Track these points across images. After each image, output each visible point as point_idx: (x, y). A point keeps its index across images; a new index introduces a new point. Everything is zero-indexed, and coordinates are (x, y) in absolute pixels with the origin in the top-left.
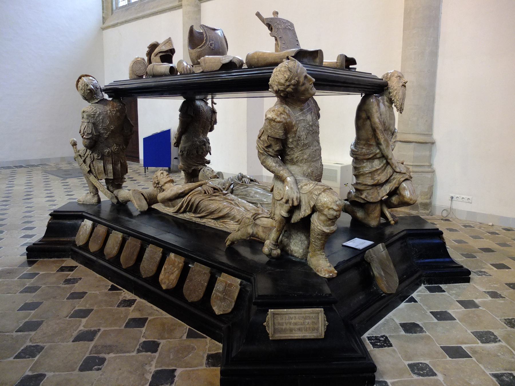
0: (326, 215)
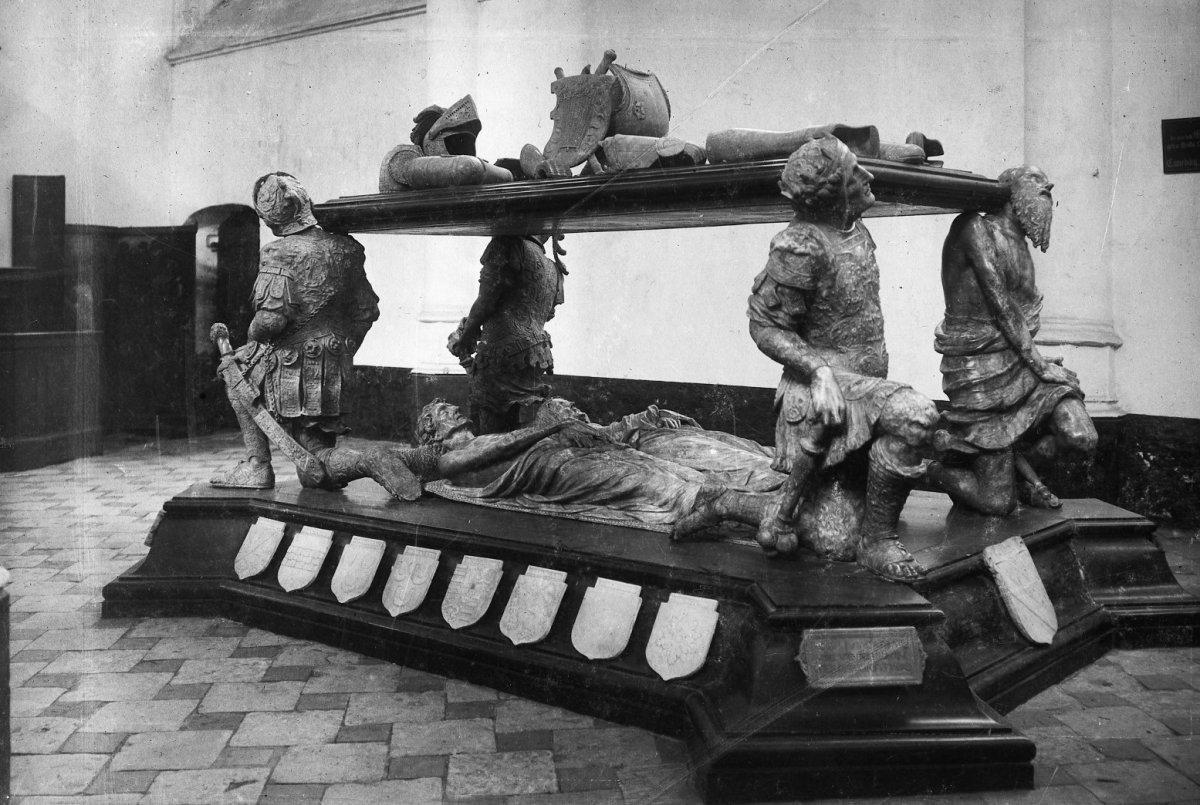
0: (902, 439)
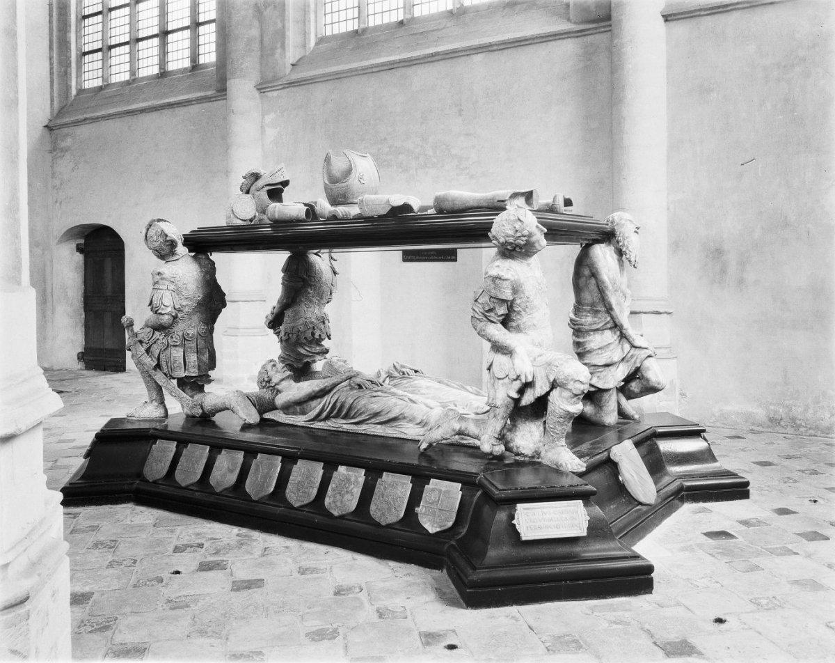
0: (570, 390)
